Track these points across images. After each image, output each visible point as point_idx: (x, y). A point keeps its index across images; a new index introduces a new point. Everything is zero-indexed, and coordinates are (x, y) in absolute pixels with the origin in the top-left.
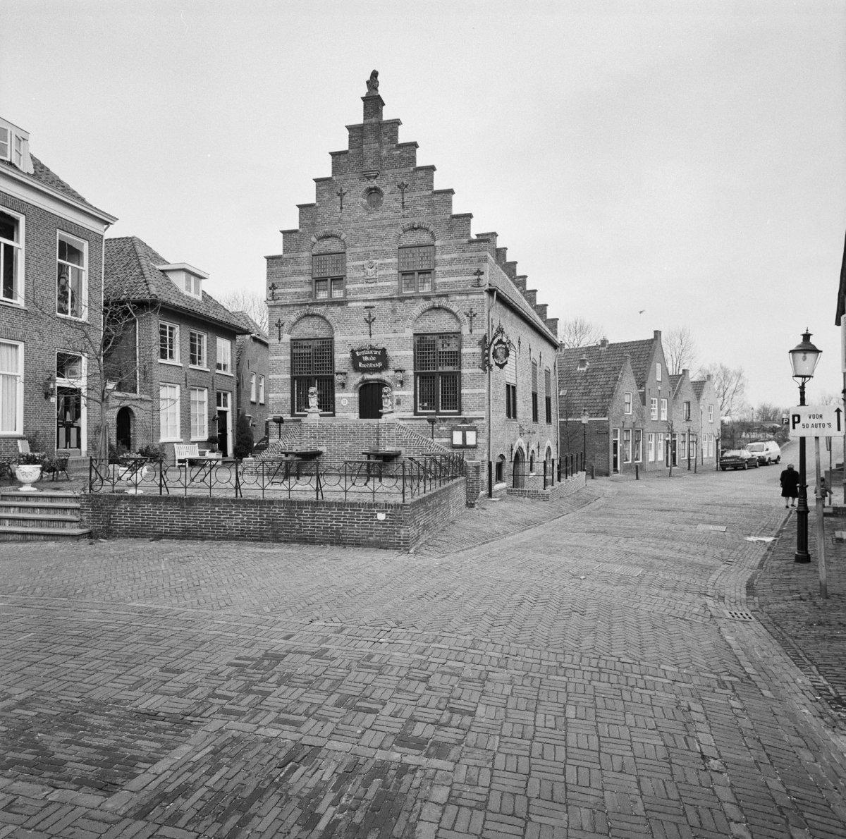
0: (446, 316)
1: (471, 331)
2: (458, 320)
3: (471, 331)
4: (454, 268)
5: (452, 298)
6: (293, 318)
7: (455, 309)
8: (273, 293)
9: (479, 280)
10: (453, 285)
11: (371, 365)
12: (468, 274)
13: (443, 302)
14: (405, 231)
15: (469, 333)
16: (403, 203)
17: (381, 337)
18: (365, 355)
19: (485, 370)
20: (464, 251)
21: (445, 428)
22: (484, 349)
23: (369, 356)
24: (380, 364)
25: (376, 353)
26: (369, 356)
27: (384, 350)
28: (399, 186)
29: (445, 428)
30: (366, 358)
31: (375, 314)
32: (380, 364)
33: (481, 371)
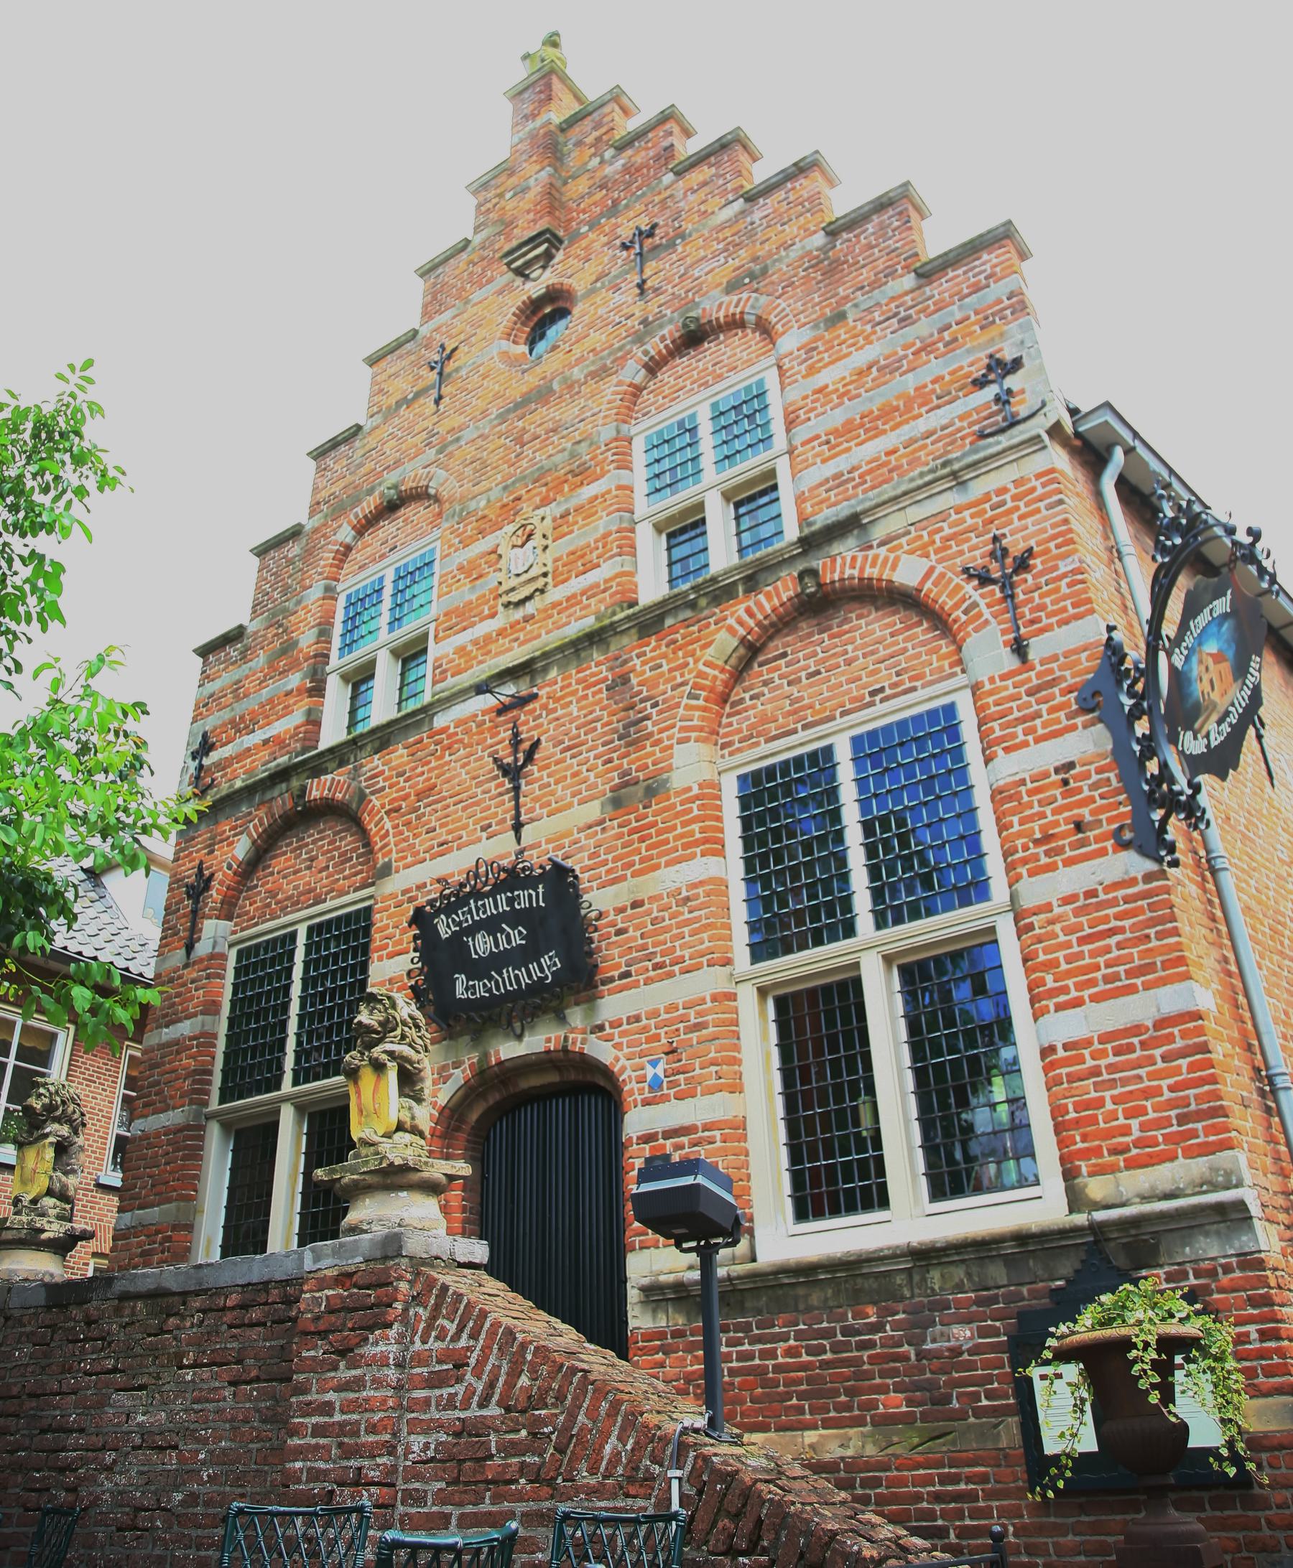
0: (872, 627)
1: (1019, 648)
2: (939, 621)
3: (1019, 648)
4: (872, 400)
5: (878, 532)
6: (241, 848)
7: (908, 573)
8: (201, 767)
9: (1003, 400)
10: (881, 469)
11: (511, 978)
12: (946, 398)
13: (843, 563)
14: (653, 367)
15: (1010, 662)
16: (641, 286)
17: (563, 824)
18: (472, 931)
19: (1154, 844)
20: (905, 321)
21: (963, 1334)
22: (1121, 725)
23: (491, 926)
24: (549, 964)
25: (524, 898)
26: (491, 926)
27: (560, 880)
28: (625, 247)
29: (963, 1334)
30: (482, 945)
31: (531, 724)
32: (549, 964)
33: (1135, 864)
